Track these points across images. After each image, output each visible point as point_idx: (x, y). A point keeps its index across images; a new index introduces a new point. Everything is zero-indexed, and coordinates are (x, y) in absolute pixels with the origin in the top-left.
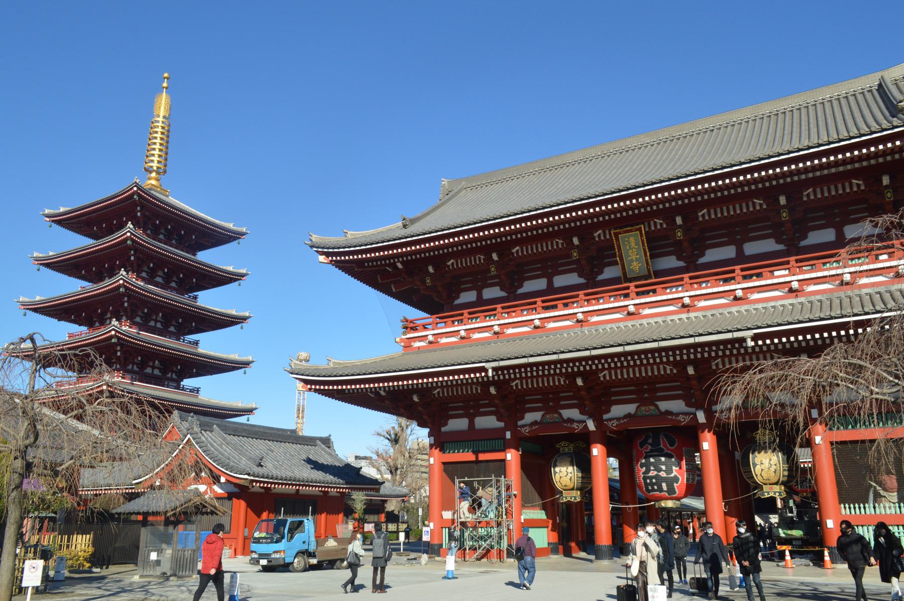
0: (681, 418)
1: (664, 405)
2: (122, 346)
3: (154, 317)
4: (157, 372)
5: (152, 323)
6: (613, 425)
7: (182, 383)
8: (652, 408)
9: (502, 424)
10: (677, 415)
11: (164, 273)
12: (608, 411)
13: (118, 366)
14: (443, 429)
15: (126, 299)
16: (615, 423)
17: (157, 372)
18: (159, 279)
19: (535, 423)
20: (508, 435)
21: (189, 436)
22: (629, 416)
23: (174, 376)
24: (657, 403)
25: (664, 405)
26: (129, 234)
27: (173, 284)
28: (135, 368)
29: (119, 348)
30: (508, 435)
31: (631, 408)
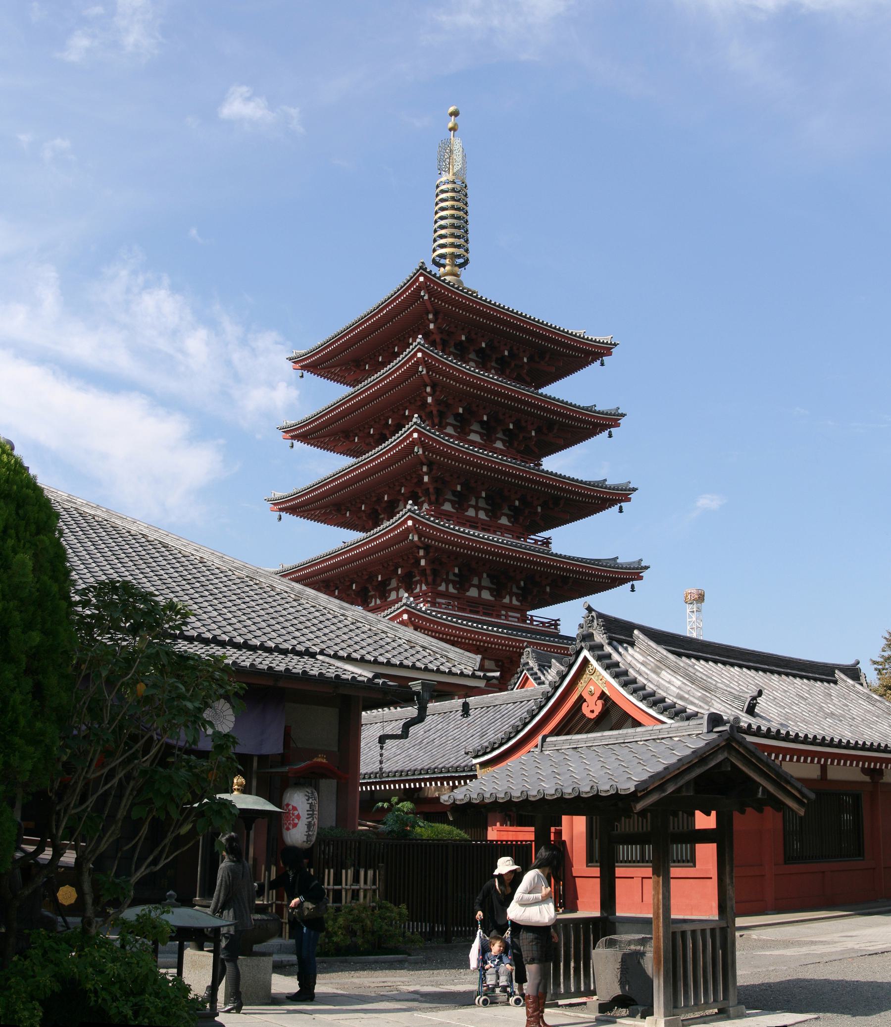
2: (427, 548)
3: (473, 502)
4: (486, 595)
5: (471, 513)
7: (528, 613)
11: (482, 422)
13: (424, 588)
15: (425, 469)
17: (486, 595)
18: (474, 437)
21: (585, 653)
23: (515, 602)
26: (419, 355)
27: (499, 445)
28: (451, 590)
29: (421, 553)
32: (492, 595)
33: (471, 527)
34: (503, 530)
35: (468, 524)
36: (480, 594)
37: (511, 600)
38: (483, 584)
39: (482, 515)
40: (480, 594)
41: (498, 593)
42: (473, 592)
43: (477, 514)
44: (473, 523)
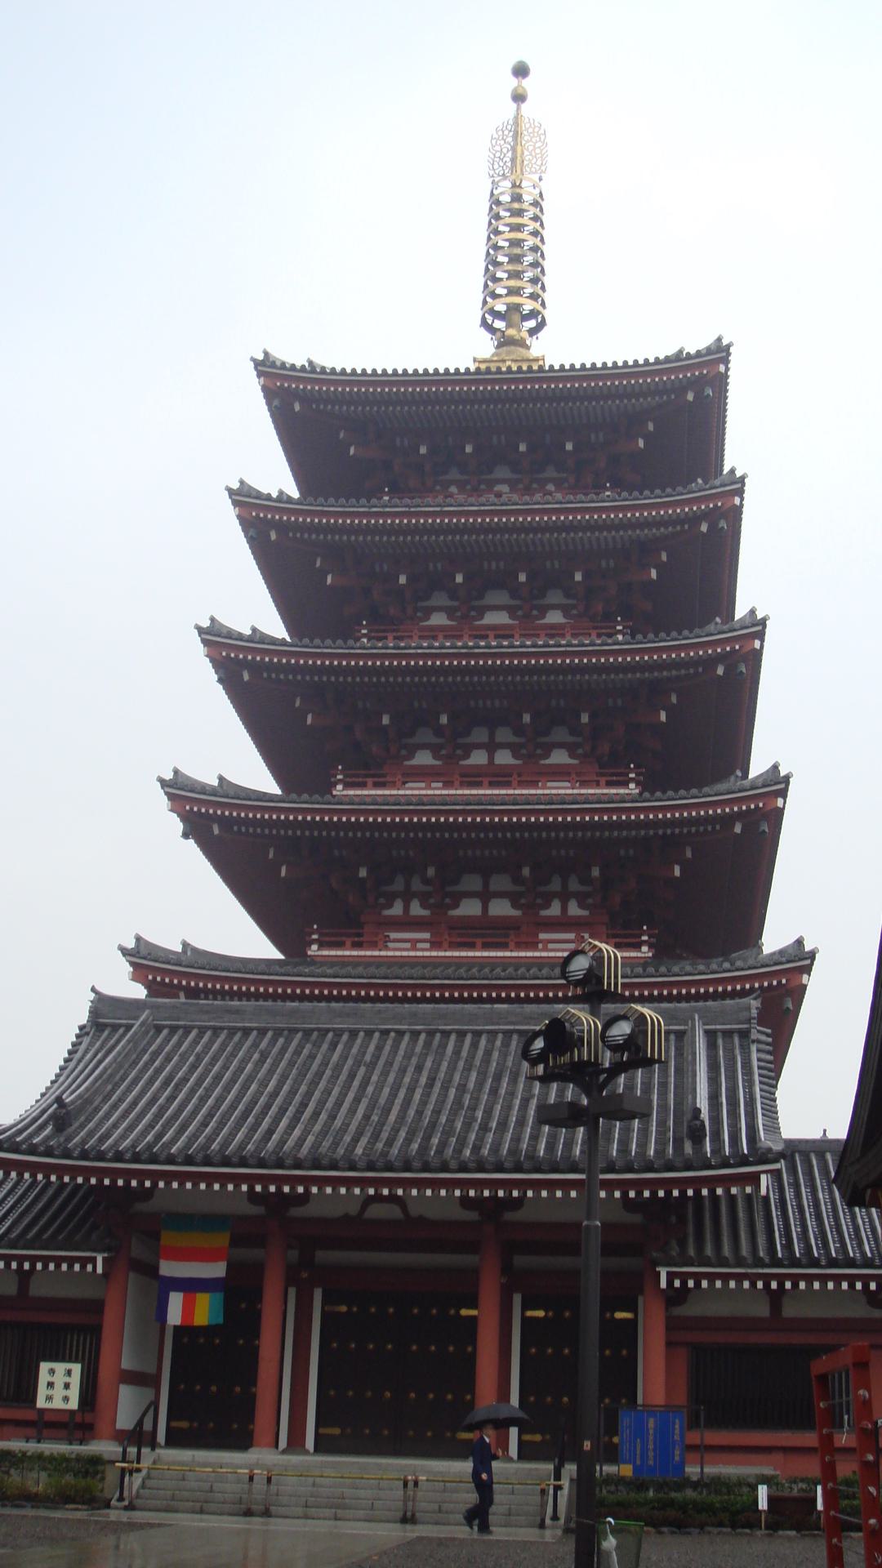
5: (478, 758)
17: (501, 908)
23: (574, 910)
28: (416, 909)
32: (515, 906)
33: (463, 785)
34: (559, 773)
35: (370, 781)
36: (485, 908)
37: (564, 909)
38: (493, 887)
39: (504, 758)
40: (485, 908)
41: (530, 898)
42: (470, 908)
43: (491, 758)
44: (473, 777)
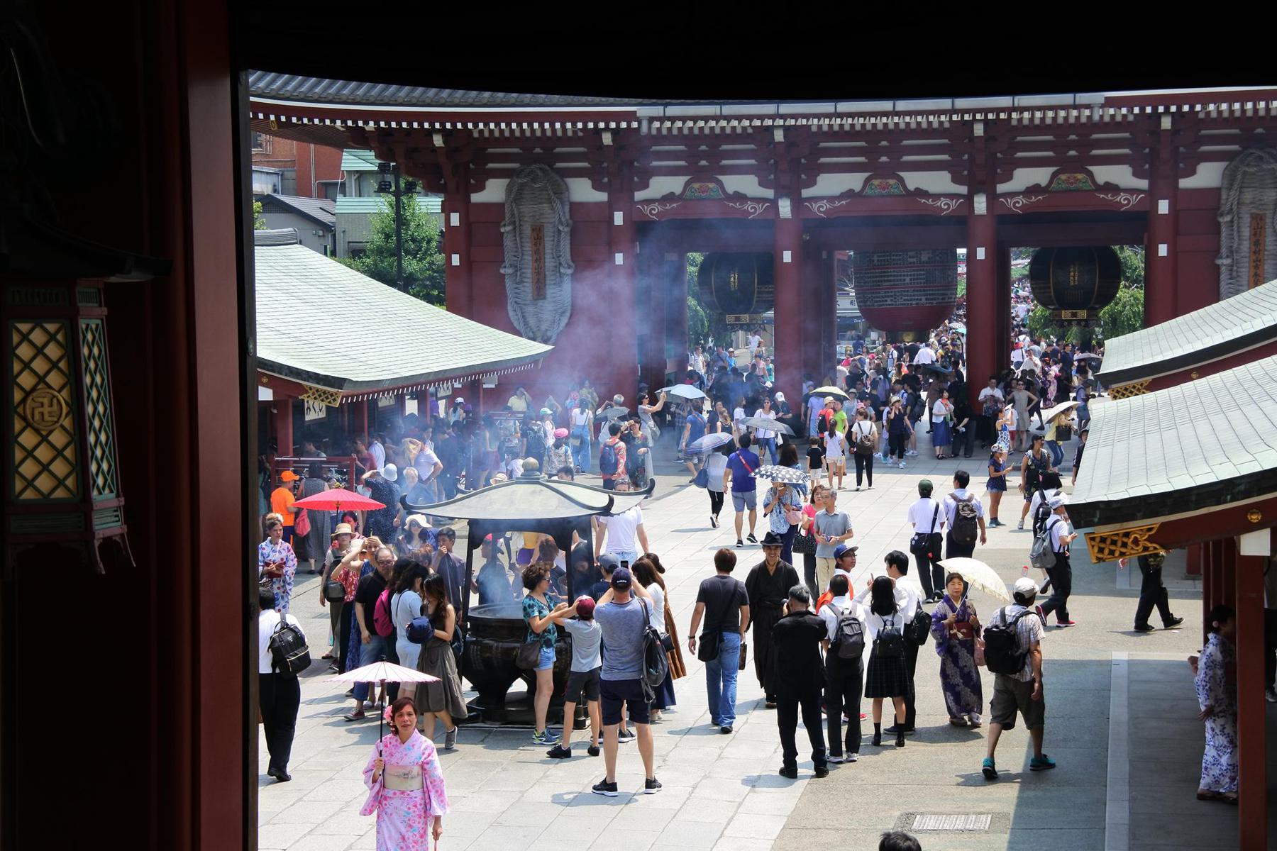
0: (942, 203)
1: (914, 180)
6: (819, 209)
8: (892, 182)
9: (603, 197)
10: (937, 196)
12: (812, 183)
14: (476, 198)
16: (825, 206)
19: (669, 198)
20: (619, 218)
22: (850, 194)
24: (902, 174)
25: (914, 180)
30: (619, 218)
31: (854, 181)
